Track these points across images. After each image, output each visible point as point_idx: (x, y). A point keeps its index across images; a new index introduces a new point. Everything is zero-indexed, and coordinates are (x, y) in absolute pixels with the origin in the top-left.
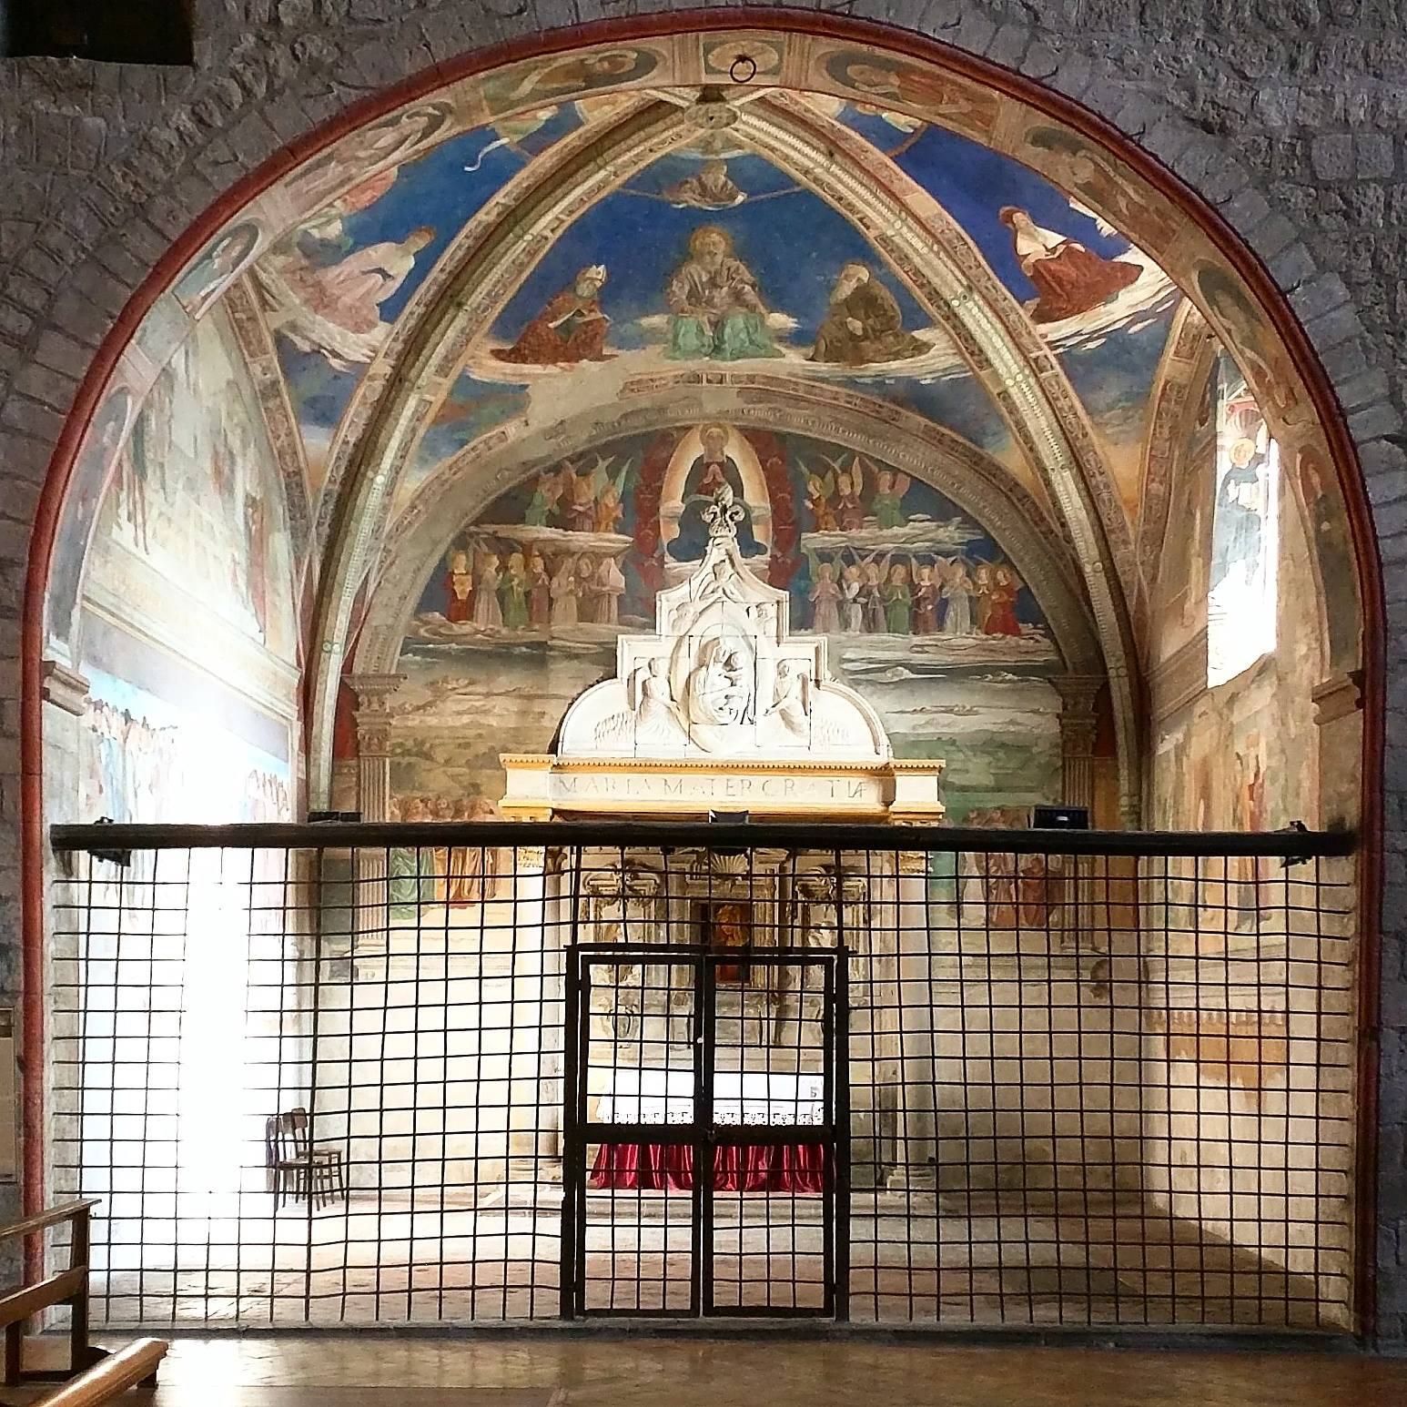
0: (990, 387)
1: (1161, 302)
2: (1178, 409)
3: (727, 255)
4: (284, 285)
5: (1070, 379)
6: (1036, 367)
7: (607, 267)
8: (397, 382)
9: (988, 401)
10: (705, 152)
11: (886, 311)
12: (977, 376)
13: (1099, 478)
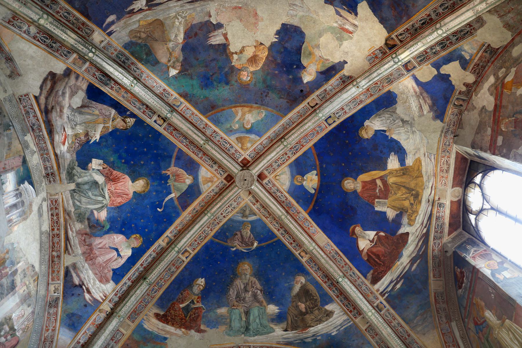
0: (361, 326)
2: (445, 306)
3: (251, 276)
4: (77, 242)
5: (394, 308)
6: (378, 309)
7: (205, 279)
8: (110, 316)
9: (363, 337)
10: (244, 216)
11: (313, 296)
12: (355, 323)
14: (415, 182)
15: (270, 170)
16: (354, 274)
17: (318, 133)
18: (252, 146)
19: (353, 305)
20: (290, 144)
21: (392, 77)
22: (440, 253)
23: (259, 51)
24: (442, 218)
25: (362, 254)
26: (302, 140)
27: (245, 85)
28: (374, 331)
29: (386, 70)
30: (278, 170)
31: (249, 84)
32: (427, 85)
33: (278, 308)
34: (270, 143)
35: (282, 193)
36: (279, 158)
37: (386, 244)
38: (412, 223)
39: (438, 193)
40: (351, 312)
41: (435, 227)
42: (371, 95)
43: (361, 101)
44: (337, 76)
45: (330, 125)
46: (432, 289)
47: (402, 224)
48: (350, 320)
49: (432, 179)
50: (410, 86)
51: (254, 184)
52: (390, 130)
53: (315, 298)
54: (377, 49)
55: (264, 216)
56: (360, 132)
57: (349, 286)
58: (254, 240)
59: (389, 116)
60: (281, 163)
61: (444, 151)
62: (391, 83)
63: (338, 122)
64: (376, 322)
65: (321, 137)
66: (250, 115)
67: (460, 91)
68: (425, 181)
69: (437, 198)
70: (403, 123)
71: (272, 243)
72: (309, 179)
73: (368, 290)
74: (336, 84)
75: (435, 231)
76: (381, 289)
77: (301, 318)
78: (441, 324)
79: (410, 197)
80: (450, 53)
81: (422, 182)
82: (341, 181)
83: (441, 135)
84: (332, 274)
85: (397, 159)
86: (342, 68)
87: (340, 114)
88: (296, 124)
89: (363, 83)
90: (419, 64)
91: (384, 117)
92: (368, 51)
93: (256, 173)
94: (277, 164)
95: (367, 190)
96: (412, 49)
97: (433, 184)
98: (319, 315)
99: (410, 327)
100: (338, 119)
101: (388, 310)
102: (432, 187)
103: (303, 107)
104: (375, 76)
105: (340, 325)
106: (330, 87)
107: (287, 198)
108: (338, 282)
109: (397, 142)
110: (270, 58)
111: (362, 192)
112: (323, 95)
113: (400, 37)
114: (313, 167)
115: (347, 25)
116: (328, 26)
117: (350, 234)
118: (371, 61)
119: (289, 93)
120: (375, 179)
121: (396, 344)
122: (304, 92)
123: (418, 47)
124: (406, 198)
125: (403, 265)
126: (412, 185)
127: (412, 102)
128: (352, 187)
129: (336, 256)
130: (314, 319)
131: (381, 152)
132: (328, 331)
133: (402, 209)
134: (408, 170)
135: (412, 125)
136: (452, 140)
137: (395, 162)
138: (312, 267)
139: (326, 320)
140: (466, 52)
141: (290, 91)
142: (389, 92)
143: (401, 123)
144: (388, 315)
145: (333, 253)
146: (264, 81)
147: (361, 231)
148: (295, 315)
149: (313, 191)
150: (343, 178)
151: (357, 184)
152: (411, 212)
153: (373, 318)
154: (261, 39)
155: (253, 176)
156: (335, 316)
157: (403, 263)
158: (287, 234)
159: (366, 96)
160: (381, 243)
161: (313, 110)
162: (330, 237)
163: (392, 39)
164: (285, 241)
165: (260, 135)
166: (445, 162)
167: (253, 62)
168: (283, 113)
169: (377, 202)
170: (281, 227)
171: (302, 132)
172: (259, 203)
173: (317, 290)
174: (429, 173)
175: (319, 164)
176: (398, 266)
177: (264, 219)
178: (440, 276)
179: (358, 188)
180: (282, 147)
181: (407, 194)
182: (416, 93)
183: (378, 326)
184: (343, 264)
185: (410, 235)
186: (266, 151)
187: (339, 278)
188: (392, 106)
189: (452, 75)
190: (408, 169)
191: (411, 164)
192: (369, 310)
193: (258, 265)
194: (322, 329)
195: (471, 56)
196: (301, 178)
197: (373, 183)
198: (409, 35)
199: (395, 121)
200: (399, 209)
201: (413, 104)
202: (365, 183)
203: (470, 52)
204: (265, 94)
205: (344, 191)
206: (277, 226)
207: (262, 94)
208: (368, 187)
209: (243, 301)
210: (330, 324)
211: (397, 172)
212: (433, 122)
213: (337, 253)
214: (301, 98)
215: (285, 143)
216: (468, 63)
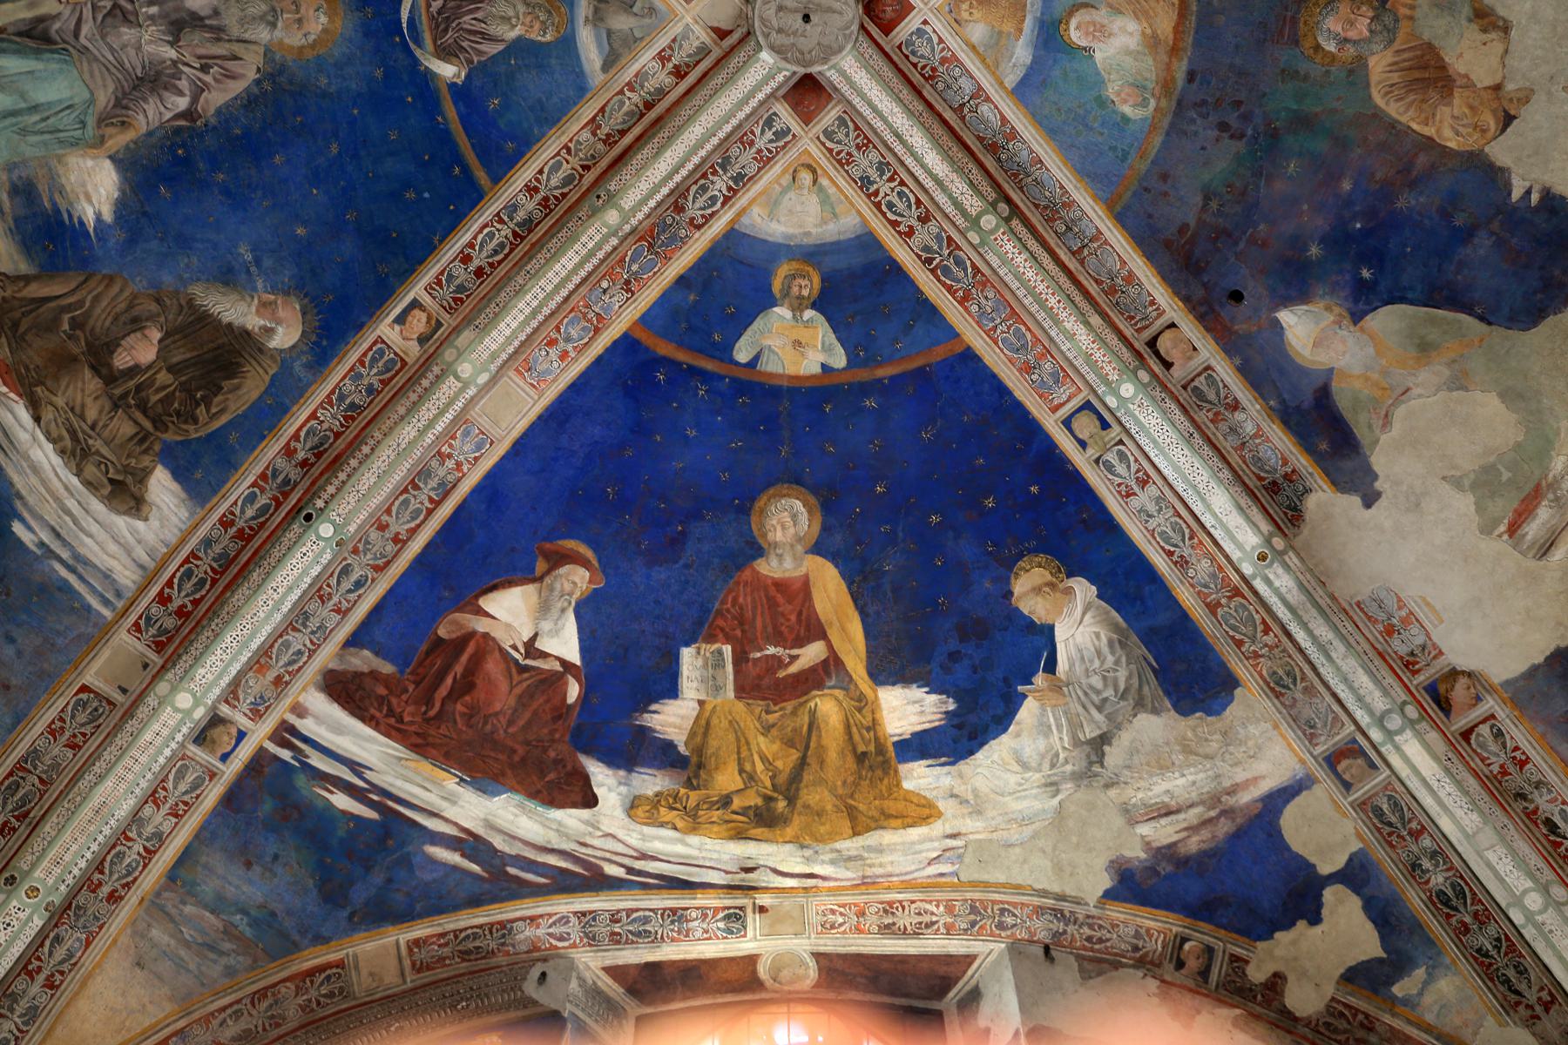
0: (96, 665)
1: (530, 865)
3: (268, 52)
5: (230, 799)
9: (46, 681)
12: (106, 630)
13: (35, 989)
14: (829, 807)
15: (841, 136)
16: (359, 584)
17: (1027, 369)
18: (973, 48)
19: (196, 603)
20: (983, 243)
21: (1299, 695)
22: (524, 948)
23: (1471, 108)
24: (679, 932)
25: (460, 610)
26: (991, 295)
27: (1294, 21)
28: (88, 730)
29: (1345, 680)
30: (841, 182)
31: (1297, 43)
32: (1270, 835)
33: (108, 216)
34: (980, 139)
35: (727, 200)
36: (902, 183)
37: (527, 715)
38: (640, 812)
39: (788, 903)
40: (163, 599)
41: (637, 910)
42: (1212, 608)
43: (1182, 564)
44: (1302, 462)
45: (1067, 423)
46: (358, 949)
47: (630, 770)
48: (120, 604)
49: (849, 874)
50: (1260, 767)
51: (784, 64)
52: (1057, 688)
53: (201, 411)
54: (1428, 635)
55: (602, 110)
56: (1041, 558)
57: (300, 578)
58: (470, 62)
59: (1122, 686)
60: (876, 193)
61: (974, 910)
62: (1272, 690)
63: (1081, 460)
64: (148, 736)
65: (1010, 385)
66: (1133, 42)
67: (1247, 962)
68: (838, 845)
69: (764, 900)
70: (1090, 742)
71: (459, 160)
72: (802, 334)
73: (290, 663)
74: (1265, 452)
75: (618, 911)
76: (307, 726)
77: (76, 350)
78: (208, 1022)
79: (758, 792)
80: (1417, 927)
81: (833, 836)
82: (798, 481)
83: (1044, 893)
84: (348, 487)
85: (927, 726)
86: (1340, 485)
87: (1120, 469)
88: (1072, 265)
89: (1284, 581)
90: (1361, 806)
91: (1117, 662)
92: (1424, 599)
93: (843, 73)
94: (874, 175)
95: (772, 604)
96: (1447, 789)
97: (824, 878)
98: (107, 443)
99: (158, 894)
100: (1097, 461)
101: (212, 775)
102: (811, 876)
103: (1153, 303)
104: (1317, 632)
105: (77, 557)
106: (1250, 428)
107: (699, 227)
108: (308, 518)
109: (1001, 721)
110: (1422, 160)
111: (760, 583)
112: (1212, 396)
113: (1484, 730)
114: (866, 350)
115: (1553, 516)
116: (1558, 434)
117: (548, 546)
118: (1373, 609)
119: (1229, 235)
120: (822, 635)
121: (67, 858)
122: (1228, 311)
123: (1459, 813)
124: (750, 778)
125: (445, 804)
126: (813, 796)
127: (1191, 778)
128: (778, 536)
129: (428, 489)
130: (82, 417)
131: (954, 656)
132: (31, 500)
133: (700, 766)
134: (879, 773)
135: (1083, 777)
136: (1021, 934)
137: (914, 719)
138: (359, 376)
139: (88, 484)
140: (1426, 984)
141: (1242, 245)
142: (1230, 683)
143: (1090, 732)
144: (190, 778)
145: (442, 472)
146: (1303, 122)
147: (571, 594)
148: (87, 315)
149: (742, 354)
150: (814, 490)
151: (795, 559)
152: (692, 803)
153: (168, 717)
154: (1532, 119)
155: (825, 60)
156: (121, 522)
157: (454, 803)
158: (515, 234)
159: (1206, 586)
160: (529, 694)
161: (1137, 345)
162: (520, 447)
163: (1478, 699)
164: (476, 227)
165: (1021, 92)
166: (927, 919)
167: (1417, 74)
168: (1127, 207)
169: (720, 652)
170: (546, 199)
171: (1042, 304)
172: (670, 80)
173: (245, 415)
174: (873, 858)
175: (880, 380)
176: (440, 785)
177: (588, 111)
178: (418, 968)
179: (774, 562)
180: (973, 204)
181: (772, 778)
182: (1232, 791)
183: (134, 752)
184: (399, 527)
185: (585, 813)
186: (940, 116)
187: (333, 523)
188: (1168, 693)
189: (1318, 930)
190: (886, 773)
191: (907, 785)
192: (205, 694)
193: (333, 89)
194: (36, 469)
195: (1406, 1002)
196: (805, 293)
197: (808, 629)
198: (1496, 769)
199: (1099, 709)
200: (699, 751)
201: (1181, 781)
202: (801, 591)
203: (1428, 999)
204: (1233, 119)
205: (753, 499)
206: (554, 182)
207: (1238, 104)
208: (786, 608)
209: (109, 14)
210: (71, 504)
211: (868, 729)
212: (1101, 862)
213: (446, 491)
214: (1199, 293)
215: (989, 221)
216: (1376, 991)
